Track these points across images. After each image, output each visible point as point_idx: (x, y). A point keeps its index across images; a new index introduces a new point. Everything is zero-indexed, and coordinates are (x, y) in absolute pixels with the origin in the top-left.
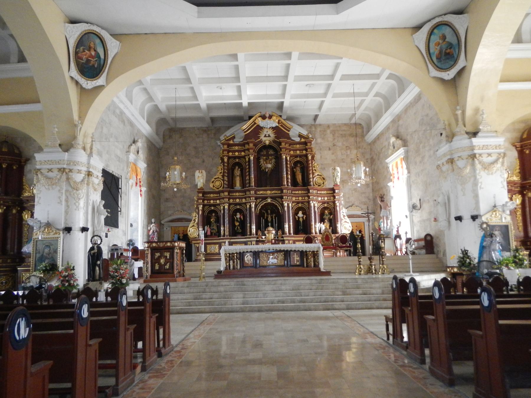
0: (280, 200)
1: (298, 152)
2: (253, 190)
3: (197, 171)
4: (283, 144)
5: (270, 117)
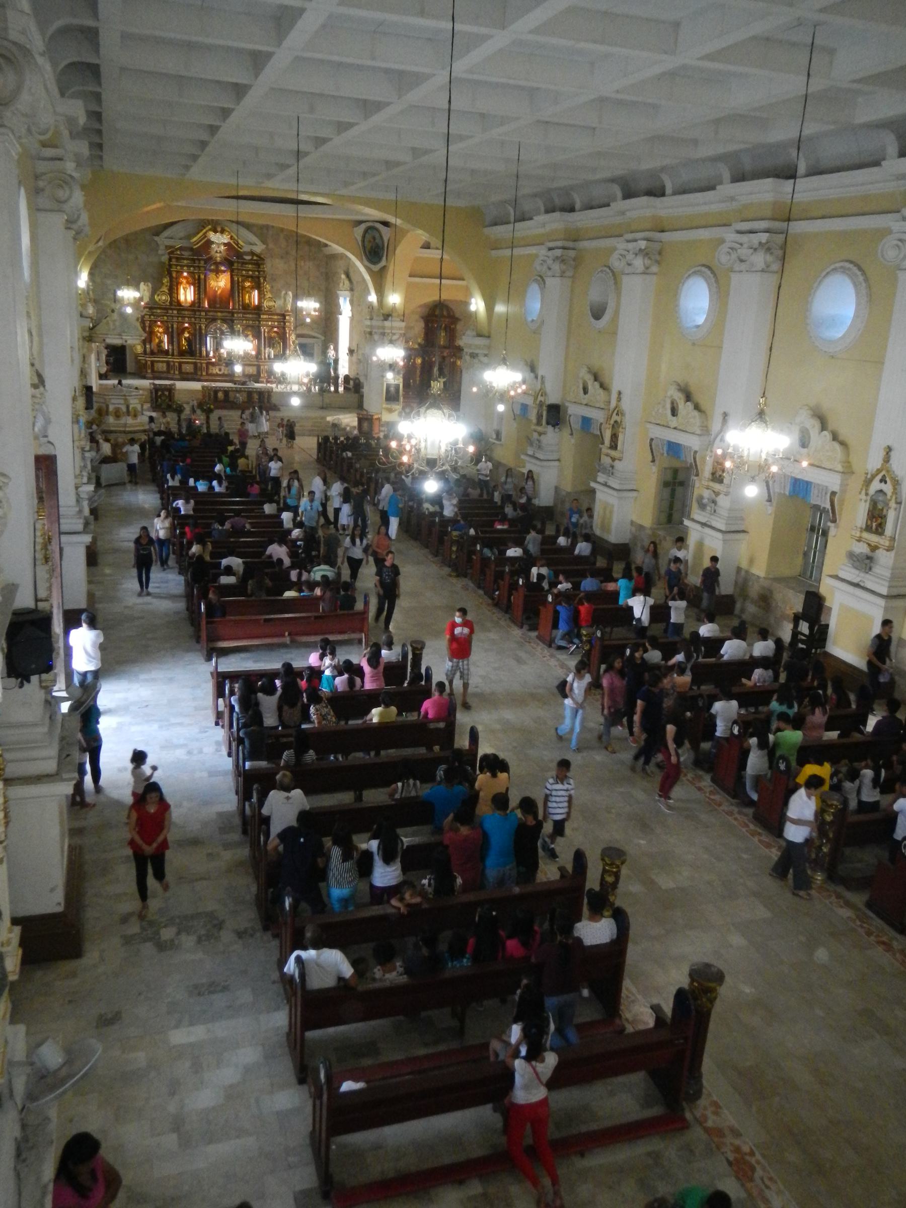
0: (230, 322)
1: (251, 273)
2: (203, 311)
3: (142, 284)
4: (236, 265)
5: (222, 232)
